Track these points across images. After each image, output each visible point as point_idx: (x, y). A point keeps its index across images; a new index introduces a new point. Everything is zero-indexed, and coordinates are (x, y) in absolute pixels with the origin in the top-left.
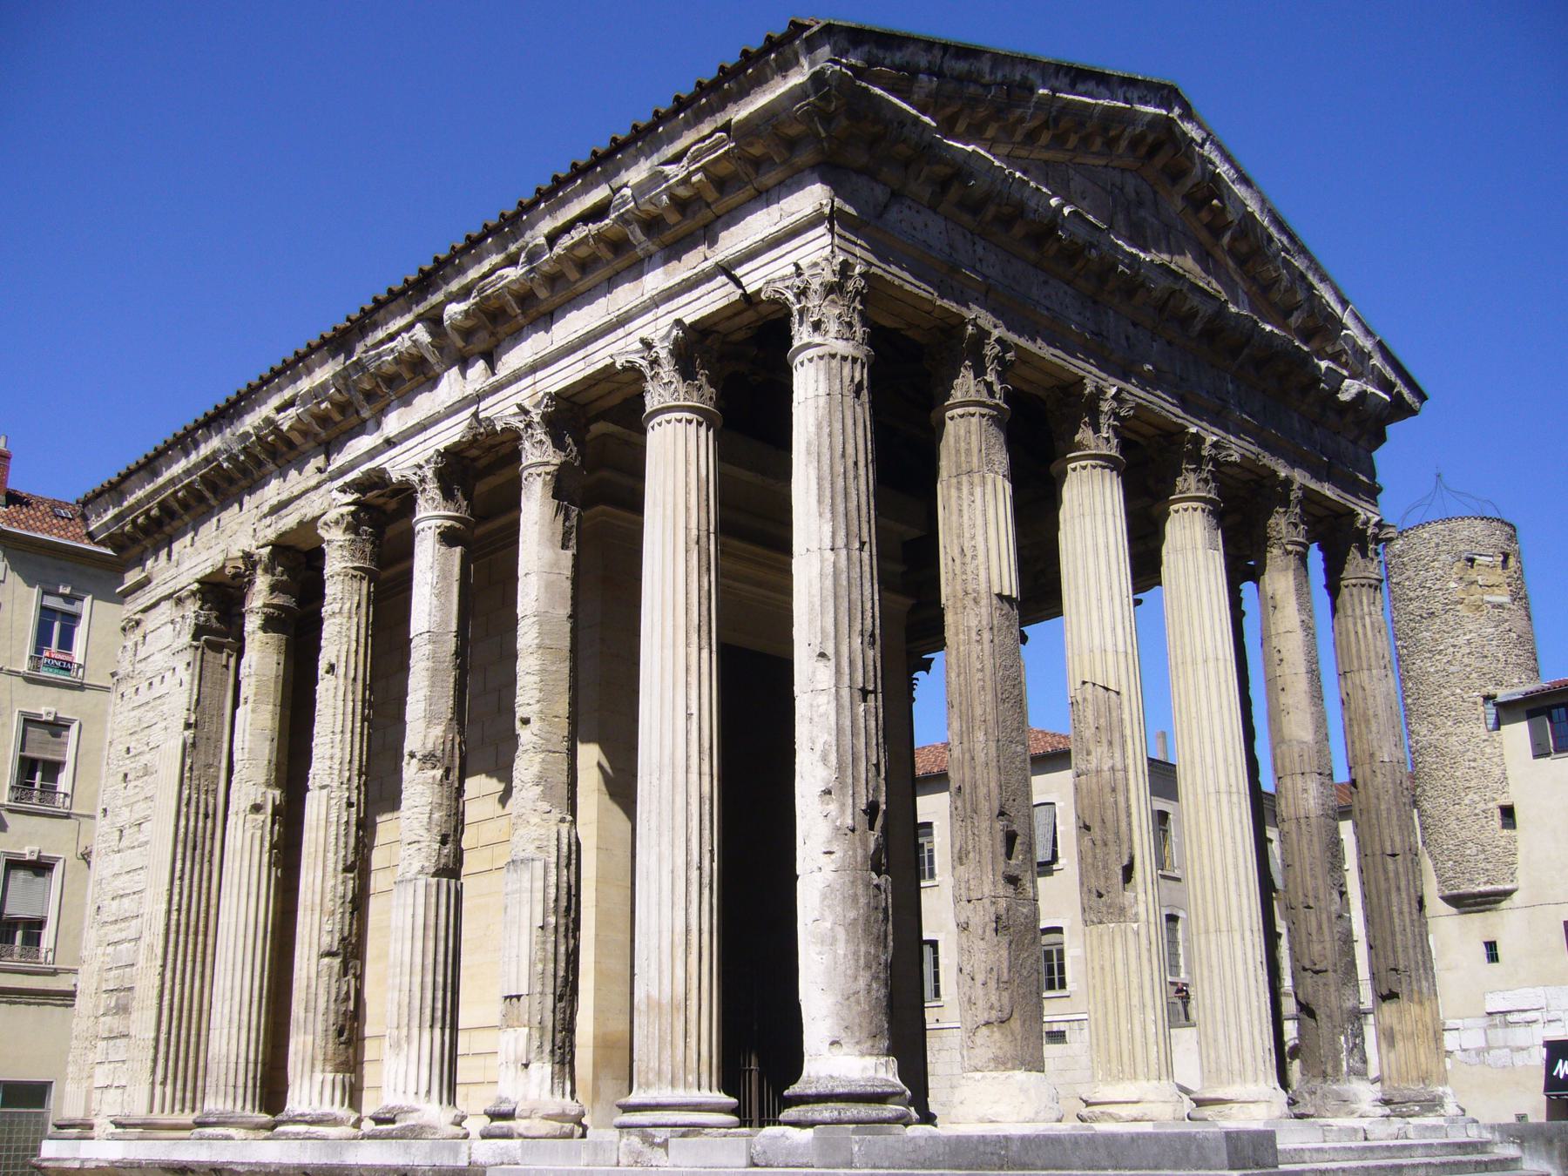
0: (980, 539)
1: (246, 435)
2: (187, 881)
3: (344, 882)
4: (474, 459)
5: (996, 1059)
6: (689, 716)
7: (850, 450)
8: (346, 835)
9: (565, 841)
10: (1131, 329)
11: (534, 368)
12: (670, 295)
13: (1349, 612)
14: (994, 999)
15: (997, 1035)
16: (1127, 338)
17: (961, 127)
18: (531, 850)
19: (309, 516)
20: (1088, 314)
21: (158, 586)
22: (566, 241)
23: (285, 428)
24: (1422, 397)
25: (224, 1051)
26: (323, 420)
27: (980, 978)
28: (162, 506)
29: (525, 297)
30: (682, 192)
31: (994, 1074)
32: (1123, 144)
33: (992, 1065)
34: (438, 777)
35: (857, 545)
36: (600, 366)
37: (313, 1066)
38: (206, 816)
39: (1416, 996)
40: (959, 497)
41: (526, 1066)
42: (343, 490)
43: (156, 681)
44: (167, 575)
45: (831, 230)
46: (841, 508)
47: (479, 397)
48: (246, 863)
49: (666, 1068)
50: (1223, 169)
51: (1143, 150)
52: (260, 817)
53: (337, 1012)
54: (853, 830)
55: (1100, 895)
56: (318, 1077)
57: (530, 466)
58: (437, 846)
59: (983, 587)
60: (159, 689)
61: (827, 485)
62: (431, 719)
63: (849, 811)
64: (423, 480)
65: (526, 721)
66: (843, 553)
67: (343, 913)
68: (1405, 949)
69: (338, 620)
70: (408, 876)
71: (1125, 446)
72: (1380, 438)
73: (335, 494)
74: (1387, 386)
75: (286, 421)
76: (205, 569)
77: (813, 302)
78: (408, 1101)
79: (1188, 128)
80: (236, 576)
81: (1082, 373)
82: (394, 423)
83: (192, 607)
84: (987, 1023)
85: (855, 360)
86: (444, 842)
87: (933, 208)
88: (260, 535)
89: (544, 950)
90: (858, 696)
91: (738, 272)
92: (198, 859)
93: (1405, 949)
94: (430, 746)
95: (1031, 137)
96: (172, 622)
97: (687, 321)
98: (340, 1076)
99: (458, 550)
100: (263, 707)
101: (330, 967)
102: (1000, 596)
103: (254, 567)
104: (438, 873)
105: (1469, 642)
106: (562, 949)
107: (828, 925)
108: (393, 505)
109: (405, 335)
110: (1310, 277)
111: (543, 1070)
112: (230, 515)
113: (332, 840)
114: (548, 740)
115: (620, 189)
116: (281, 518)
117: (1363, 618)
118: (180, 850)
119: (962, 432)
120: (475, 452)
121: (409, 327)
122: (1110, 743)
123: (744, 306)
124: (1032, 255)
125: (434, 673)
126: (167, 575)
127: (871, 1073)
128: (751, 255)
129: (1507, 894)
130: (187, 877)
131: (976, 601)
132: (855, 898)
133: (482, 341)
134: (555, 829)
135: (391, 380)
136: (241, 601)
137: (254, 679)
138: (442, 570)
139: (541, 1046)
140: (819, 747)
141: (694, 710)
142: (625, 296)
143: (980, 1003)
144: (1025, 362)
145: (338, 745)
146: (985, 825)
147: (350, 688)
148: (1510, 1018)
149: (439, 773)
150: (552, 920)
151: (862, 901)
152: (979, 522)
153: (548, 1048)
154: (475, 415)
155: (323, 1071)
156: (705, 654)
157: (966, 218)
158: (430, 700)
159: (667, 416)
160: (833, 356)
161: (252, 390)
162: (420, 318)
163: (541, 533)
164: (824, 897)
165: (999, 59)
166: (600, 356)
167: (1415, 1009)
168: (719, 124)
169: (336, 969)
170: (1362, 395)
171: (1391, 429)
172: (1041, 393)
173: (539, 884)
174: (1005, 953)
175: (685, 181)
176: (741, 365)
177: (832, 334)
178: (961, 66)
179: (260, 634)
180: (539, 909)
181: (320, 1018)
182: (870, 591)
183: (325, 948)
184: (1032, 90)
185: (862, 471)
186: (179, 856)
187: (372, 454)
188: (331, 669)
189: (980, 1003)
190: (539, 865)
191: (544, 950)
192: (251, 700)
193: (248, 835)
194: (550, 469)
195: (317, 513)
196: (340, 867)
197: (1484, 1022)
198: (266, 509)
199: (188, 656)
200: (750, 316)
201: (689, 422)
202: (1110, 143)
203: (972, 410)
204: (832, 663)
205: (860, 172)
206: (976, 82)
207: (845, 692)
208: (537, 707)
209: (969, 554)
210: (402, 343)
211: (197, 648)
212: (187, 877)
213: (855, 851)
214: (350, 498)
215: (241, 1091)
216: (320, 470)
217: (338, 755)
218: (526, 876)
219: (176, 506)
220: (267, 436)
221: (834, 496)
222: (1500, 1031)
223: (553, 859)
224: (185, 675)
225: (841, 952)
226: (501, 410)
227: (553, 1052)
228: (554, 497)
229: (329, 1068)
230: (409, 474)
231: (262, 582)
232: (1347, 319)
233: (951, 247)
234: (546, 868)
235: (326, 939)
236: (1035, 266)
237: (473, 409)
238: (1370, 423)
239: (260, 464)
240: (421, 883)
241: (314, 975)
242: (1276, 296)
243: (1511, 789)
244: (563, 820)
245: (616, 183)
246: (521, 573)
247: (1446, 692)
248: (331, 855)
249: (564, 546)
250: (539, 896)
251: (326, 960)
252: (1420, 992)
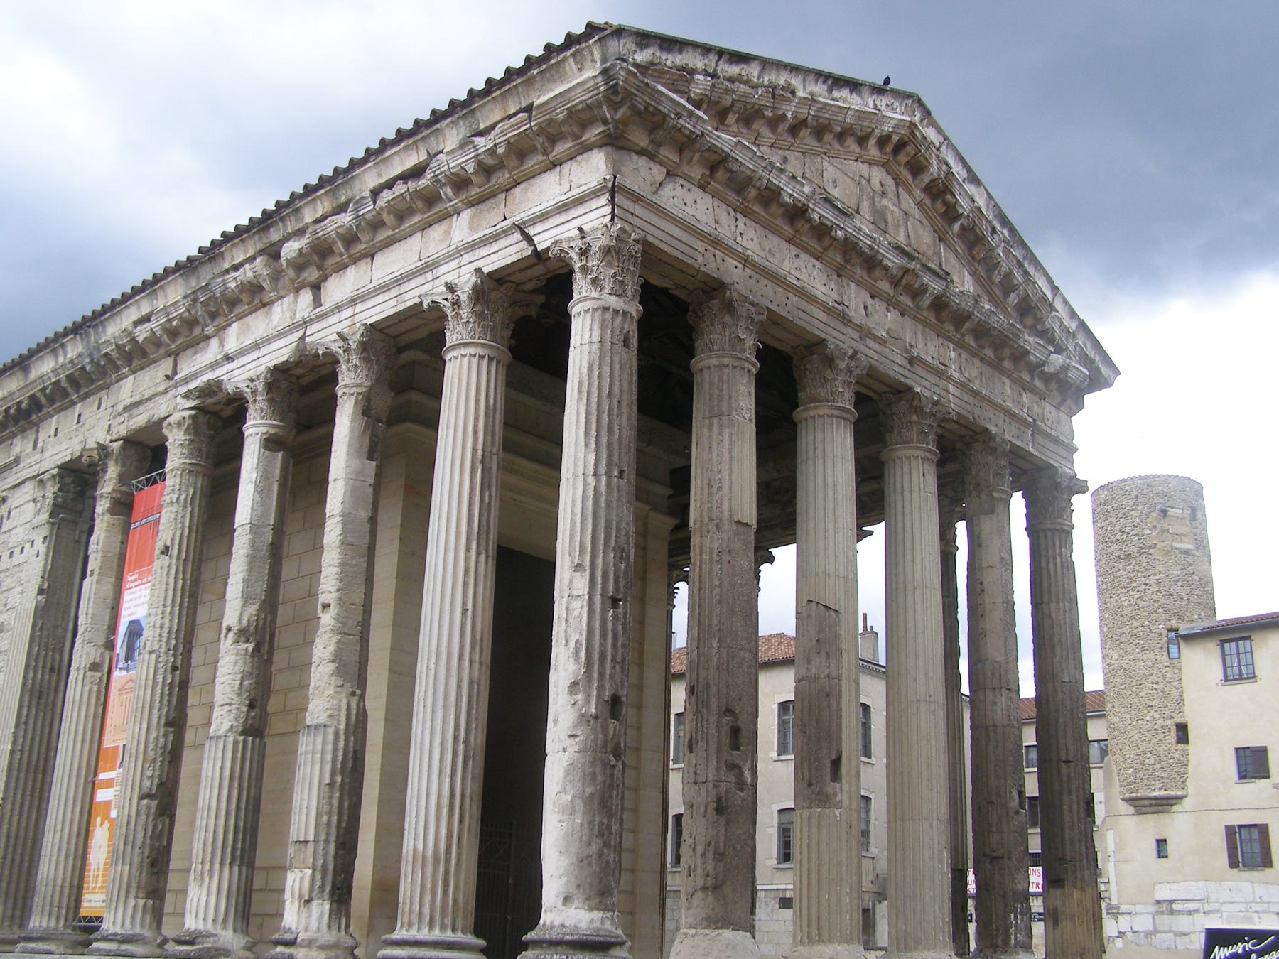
0: (726, 474)
2: (31, 726)
3: (165, 735)
4: (299, 377)
5: (708, 919)
6: (465, 611)
7: (616, 390)
8: (170, 695)
9: (354, 712)
10: (869, 301)
11: (353, 302)
12: (473, 246)
13: (1043, 553)
14: (710, 867)
15: (711, 899)
16: (866, 308)
17: (731, 119)
18: (323, 719)
19: (156, 417)
20: (832, 286)
21: (23, 468)
22: (386, 195)
23: (140, 339)
24: (1117, 373)
25: (52, 876)
26: (173, 334)
27: (700, 849)
28: (33, 398)
29: (350, 239)
30: (490, 161)
31: (707, 931)
32: (872, 142)
33: (705, 923)
34: (251, 649)
35: (616, 473)
36: (409, 304)
37: (128, 892)
38: (52, 670)
39: (1079, 883)
40: (710, 437)
41: (308, 902)
42: (186, 396)
43: (17, 550)
44: (31, 460)
45: (612, 201)
46: (604, 440)
47: (305, 323)
48: (83, 713)
49: (427, 911)
50: (957, 169)
51: (889, 148)
52: (99, 674)
53: (152, 847)
54: (596, 718)
55: (810, 784)
56: (132, 902)
57: (346, 386)
58: (245, 709)
59: (726, 514)
60: (18, 558)
61: (594, 420)
62: (247, 599)
63: (594, 701)
64: (254, 392)
65: (326, 606)
66: (604, 479)
67: (162, 762)
68: (1072, 842)
69: (174, 509)
70: (220, 733)
71: (861, 399)
72: (1080, 406)
73: (179, 399)
74: (1087, 361)
75: (142, 333)
76: (65, 456)
77: (593, 262)
78: (210, 926)
79: (931, 134)
80: (91, 465)
81: (823, 336)
82: (234, 338)
83: (51, 489)
84: (704, 888)
85: (625, 313)
86: (251, 706)
87: (703, 187)
88: (114, 430)
89: (331, 804)
90: (609, 603)
91: (531, 231)
92: (42, 707)
93: (1072, 842)
94: (245, 622)
95: (794, 130)
96: (34, 500)
97: (486, 270)
98: (150, 902)
99: (280, 455)
100: (107, 579)
101: (148, 807)
102: (738, 522)
103: (106, 456)
104: (244, 732)
105: (1158, 581)
106: (346, 804)
107: (569, 797)
108: (228, 412)
109: (248, 266)
110: (1026, 265)
111: (322, 908)
112: (87, 409)
113: (158, 698)
114: (345, 624)
115: (437, 154)
116: (131, 416)
117: (1055, 558)
118: (27, 698)
119: (716, 380)
120: (299, 371)
121: (253, 259)
122: (828, 655)
123: (535, 261)
124: (787, 229)
125: (252, 560)
126: (31, 460)
127: (598, 924)
128: (543, 217)
130: (31, 722)
131: (718, 526)
132: (593, 776)
133: (312, 274)
134: (345, 701)
135: (233, 303)
136: (94, 486)
137: (100, 555)
138: (265, 471)
139: (322, 887)
140: (572, 644)
141: (470, 606)
142: (433, 242)
143: (699, 871)
144: (775, 323)
145: (168, 616)
146: (713, 719)
147: (181, 568)
149: (251, 646)
150: (339, 779)
151: (600, 778)
152: (726, 458)
153: (328, 889)
154: (303, 338)
155: (137, 897)
156: (483, 558)
157: (732, 196)
158: (247, 582)
159: (463, 351)
160: (606, 309)
161: (115, 304)
162: (261, 252)
163: (350, 445)
164: (567, 773)
165: (766, 63)
166: (411, 295)
167: (1076, 894)
168: (523, 105)
169: (153, 810)
170: (1065, 368)
171: (1088, 398)
172: (788, 350)
173: (330, 747)
174: (722, 829)
175: (492, 152)
176: (529, 314)
177: (607, 290)
178: (734, 70)
179: (108, 516)
180: (328, 768)
181: (137, 851)
182: (625, 515)
183: (145, 790)
184: (793, 93)
185: (625, 411)
186: (26, 704)
187: (214, 365)
188: (166, 551)
189: (699, 871)
190: (331, 731)
191: (331, 804)
192: (96, 572)
193: (87, 689)
194: (363, 390)
195: (163, 415)
196: (163, 722)
197: (1153, 908)
198: (120, 408)
199: (45, 531)
200: (539, 270)
201: (482, 357)
202: (862, 141)
203: (726, 361)
204: (588, 573)
205: (641, 152)
206: (746, 83)
207: (598, 599)
208: (335, 595)
209: (715, 486)
210: (247, 273)
211: (53, 524)
212: (31, 722)
213: (596, 735)
214: (192, 404)
215: (64, 911)
216: (168, 377)
217: (167, 625)
218: (320, 739)
219: (43, 400)
220: (124, 345)
221: (599, 431)
222: (1166, 917)
223: (342, 727)
224: (41, 547)
225: (578, 821)
226: (324, 336)
227: (332, 894)
228: (364, 414)
229: (141, 895)
230: (242, 386)
231: (112, 471)
232: (1058, 305)
233: (717, 222)
234: (336, 734)
235: (147, 783)
236: (789, 241)
237: (300, 334)
238: (1070, 393)
239: (117, 368)
240: (231, 740)
241: (134, 814)
242: (997, 278)
243: (1186, 709)
244: (353, 694)
245: (434, 145)
246: (331, 478)
247: (1136, 624)
248: (155, 711)
249: (370, 458)
250: (329, 757)
251: (145, 802)
252: (1082, 880)
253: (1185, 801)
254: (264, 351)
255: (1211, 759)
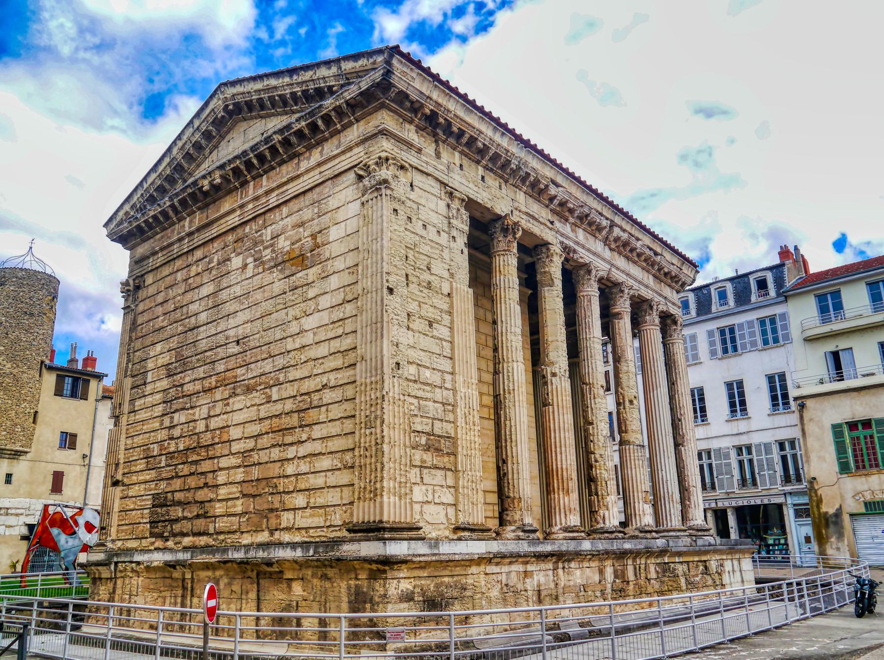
1: (526, 164)
75: (553, 190)
121: (607, 219)
129: (26, 452)
148: (10, 511)
162: (612, 221)
247: (28, 352)
253: (28, 455)
254: (595, 258)
255: (46, 435)
